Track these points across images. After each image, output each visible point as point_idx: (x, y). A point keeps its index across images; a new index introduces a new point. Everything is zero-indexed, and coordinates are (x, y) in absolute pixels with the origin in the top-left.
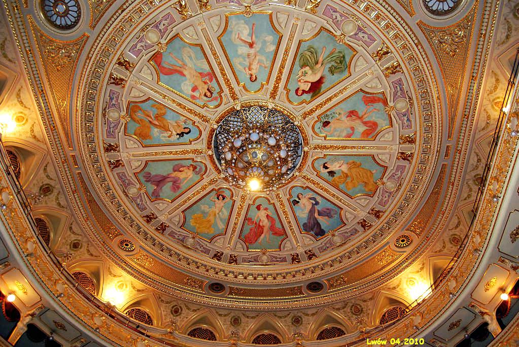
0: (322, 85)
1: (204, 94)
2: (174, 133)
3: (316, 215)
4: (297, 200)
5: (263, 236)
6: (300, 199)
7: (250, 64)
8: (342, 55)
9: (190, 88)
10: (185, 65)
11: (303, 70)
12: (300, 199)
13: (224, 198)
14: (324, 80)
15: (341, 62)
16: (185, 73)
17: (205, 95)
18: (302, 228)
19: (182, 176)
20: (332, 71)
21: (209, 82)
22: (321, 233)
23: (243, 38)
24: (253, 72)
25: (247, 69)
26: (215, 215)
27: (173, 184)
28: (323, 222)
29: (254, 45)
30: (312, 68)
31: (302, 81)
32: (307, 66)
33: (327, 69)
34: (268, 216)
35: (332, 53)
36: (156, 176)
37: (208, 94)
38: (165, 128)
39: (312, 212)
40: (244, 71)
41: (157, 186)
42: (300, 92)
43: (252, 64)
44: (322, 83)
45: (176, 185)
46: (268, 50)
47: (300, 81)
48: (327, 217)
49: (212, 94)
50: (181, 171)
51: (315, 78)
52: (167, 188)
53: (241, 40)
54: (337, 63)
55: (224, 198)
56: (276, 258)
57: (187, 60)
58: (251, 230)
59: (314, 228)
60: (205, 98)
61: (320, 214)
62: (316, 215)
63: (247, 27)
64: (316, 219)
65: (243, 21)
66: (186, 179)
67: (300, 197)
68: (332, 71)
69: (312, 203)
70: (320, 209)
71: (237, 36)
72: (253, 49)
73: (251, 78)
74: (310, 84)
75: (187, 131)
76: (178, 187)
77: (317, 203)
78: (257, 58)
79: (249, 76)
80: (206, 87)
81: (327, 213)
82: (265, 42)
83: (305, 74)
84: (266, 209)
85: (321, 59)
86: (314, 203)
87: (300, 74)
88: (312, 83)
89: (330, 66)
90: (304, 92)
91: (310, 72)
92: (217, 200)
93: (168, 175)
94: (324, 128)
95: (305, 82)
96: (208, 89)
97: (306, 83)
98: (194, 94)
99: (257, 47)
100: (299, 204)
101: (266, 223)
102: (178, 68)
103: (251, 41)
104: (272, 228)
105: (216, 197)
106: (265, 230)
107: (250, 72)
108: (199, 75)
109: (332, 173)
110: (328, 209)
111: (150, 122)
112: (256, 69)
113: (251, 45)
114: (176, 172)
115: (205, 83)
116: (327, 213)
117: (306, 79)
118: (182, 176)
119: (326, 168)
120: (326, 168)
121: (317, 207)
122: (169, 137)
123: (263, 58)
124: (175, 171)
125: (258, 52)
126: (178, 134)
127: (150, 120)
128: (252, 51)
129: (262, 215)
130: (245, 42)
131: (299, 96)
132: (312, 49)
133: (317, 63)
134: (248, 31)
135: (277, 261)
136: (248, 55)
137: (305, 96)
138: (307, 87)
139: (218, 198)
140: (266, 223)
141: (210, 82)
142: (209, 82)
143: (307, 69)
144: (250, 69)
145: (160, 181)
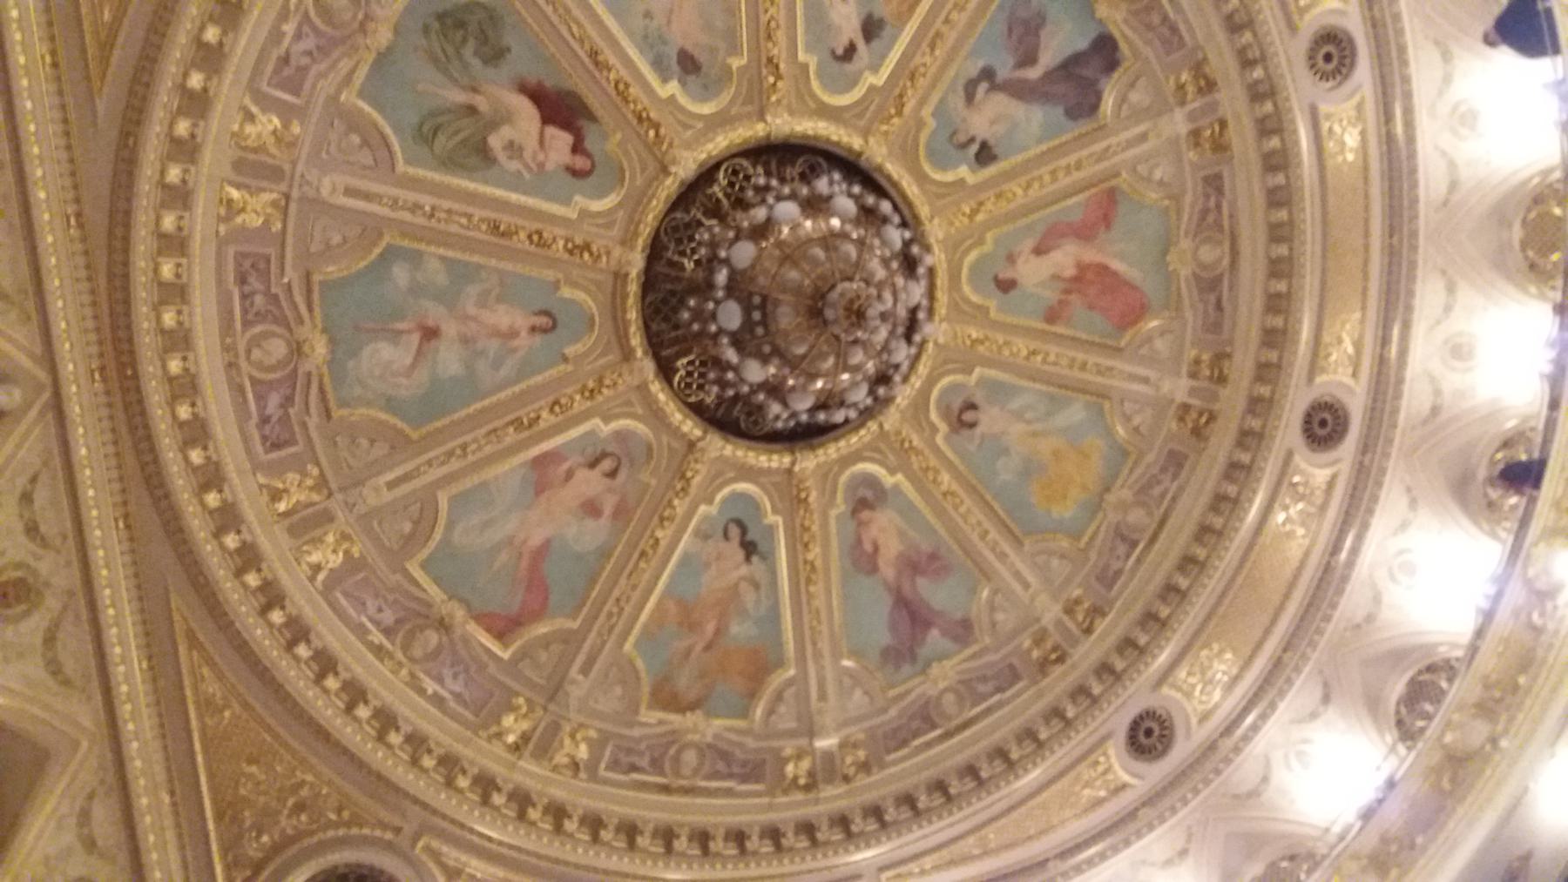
0: (548, 84)
1: (607, 481)
2: (744, 570)
3: (1034, 73)
4: (974, 148)
5: (1117, 265)
6: (972, 140)
7: (496, 333)
8: (436, 25)
9: (590, 523)
10: (510, 541)
11: (502, 157)
12: (972, 140)
13: (972, 406)
14: (532, 80)
15: (461, 25)
16: (536, 540)
17: (612, 474)
18: (1084, 126)
19: (891, 548)
20: (495, 55)
21: (565, 466)
22: (1105, 51)
23: (408, 361)
24: (522, 321)
26: (1034, 434)
27: (923, 573)
28: (1061, 41)
29: (430, 323)
30: (494, 125)
31: (541, 157)
32: (484, 141)
33: (490, 72)
34: (1039, 251)
35: (435, 60)
36: (893, 627)
37: (607, 465)
38: (729, 602)
39: (1020, 91)
41: (928, 625)
42: (580, 162)
44: (540, 84)
45: (918, 564)
47: (541, 166)
48: (1043, 34)
49: (605, 455)
50: (876, 549)
51: (527, 113)
52: (937, 594)
53: (413, 366)
54: (464, 40)
55: (972, 406)
56: (1205, 212)
57: (496, 535)
58: (1091, 307)
59: (1080, 81)
60: (622, 476)
61: (1029, 59)
62: (1034, 73)
63: (366, 352)
64: (1049, 76)
65: (351, 364)
66: (901, 534)
67: (962, 138)
68: (495, 55)
69: (988, 91)
70: (1011, 61)
71: (404, 381)
72: (444, 327)
73: (545, 331)
74: (551, 131)
75: (734, 531)
76: (933, 557)
77: (988, 74)
78: (471, 310)
79: (538, 339)
80: (582, 474)
81: (1025, 34)
82: (416, 290)
83: (513, 148)
84: (1011, 259)
85: (459, 97)
86: (983, 87)
87: (514, 165)
88: (546, 120)
89: (476, 63)
90: (577, 148)
91: (506, 132)
92: (978, 430)
93: (889, 589)
94: (704, 69)
95: (541, 142)
96: (593, 465)
97: (547, 143)
98: (608, 509)
99: (434, 312)
100: (992, 142)
101: (1065, 258)
102: (524, 563)
103: (415, 338)
104: (1084, 232)
105: (966, 432)
106: (1091, 255)
108: (543, 498)
109: (871, 28)
110: (1010, 30)
111: (708, 648)
113: (430, 333)
114: (881, 562)
115: (569, 475)
116: (1025, 34)
117: (531, 144)
118: (891, 548)
119: (851, 50)
120: (851, 50)
121: (1004, 72)
122: (757, 586)
123: (473, 290)
124: (873, 569)
126: (748, 558)
127: (699, 648)
128: (450, 329)
129: (1033, 272)
131: (593, 165)
132: (425, 129)
133: (472, 110)
135: (1219, 206)
136: (465, 340)
137: (590, 143)
138: (561, 140)
139: (972, 425)
140: (1065, 258)
141: (566, 459)
142: (565, 466)
143: (495, 142)
145: (913, 617)
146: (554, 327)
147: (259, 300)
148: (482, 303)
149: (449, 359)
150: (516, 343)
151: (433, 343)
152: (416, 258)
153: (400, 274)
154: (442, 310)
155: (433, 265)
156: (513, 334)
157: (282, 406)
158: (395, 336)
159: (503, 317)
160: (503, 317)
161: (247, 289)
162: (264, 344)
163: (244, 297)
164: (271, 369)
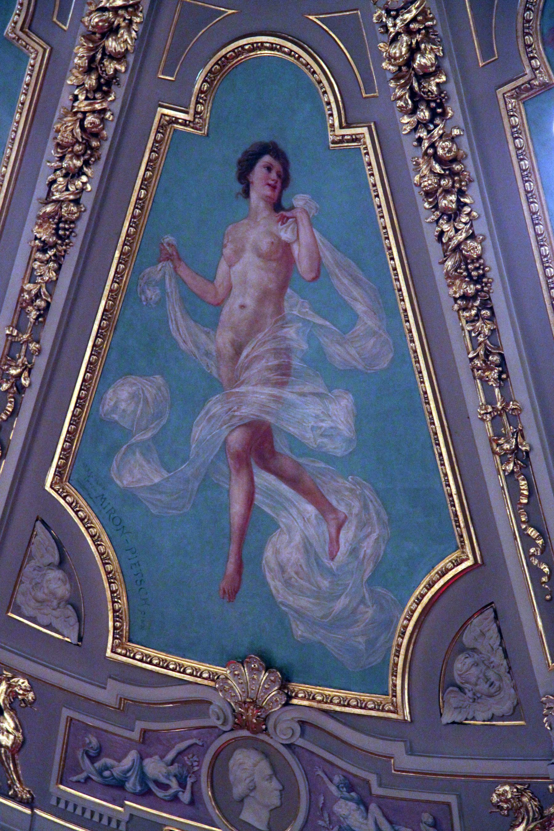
7: (274, 297)
23: (310, 509)
24: (258, 231)
25: (304, 265)
29: (237, 439)
40: (328, 257)
43: (264, 297)
46: (152, 387)
71: (347, 536)
72: (247, 411)
78: (224, 338)
79: (299, 200)
82: (168, 448)
99: (213, 429)
103: (264, 479)
107: (286, 235)
112: (238, 253)
113: (260, 445)
123: (182, 329)
125: (214, 386)
128: (255, 397)
130: (294, 482)
134: (269, 553)
136: (283, 374)
144: (283, 255)
146: (270, 149)
147: (155, 767)
148: (206, 309)
149: (319, 419)
150: (301, 253)
151: (280, 445)
152: (98, 436)
153: (136, 473)
154: (215, 406)
155: (121, 398)
156: (282, 256)
157: (363, 805)
158: (254, 525)
159: (245, 274)
160: (245, 274)
161: (131, 785)
162: (238, 791)
163: (144, 795)
164: (288, 792)
